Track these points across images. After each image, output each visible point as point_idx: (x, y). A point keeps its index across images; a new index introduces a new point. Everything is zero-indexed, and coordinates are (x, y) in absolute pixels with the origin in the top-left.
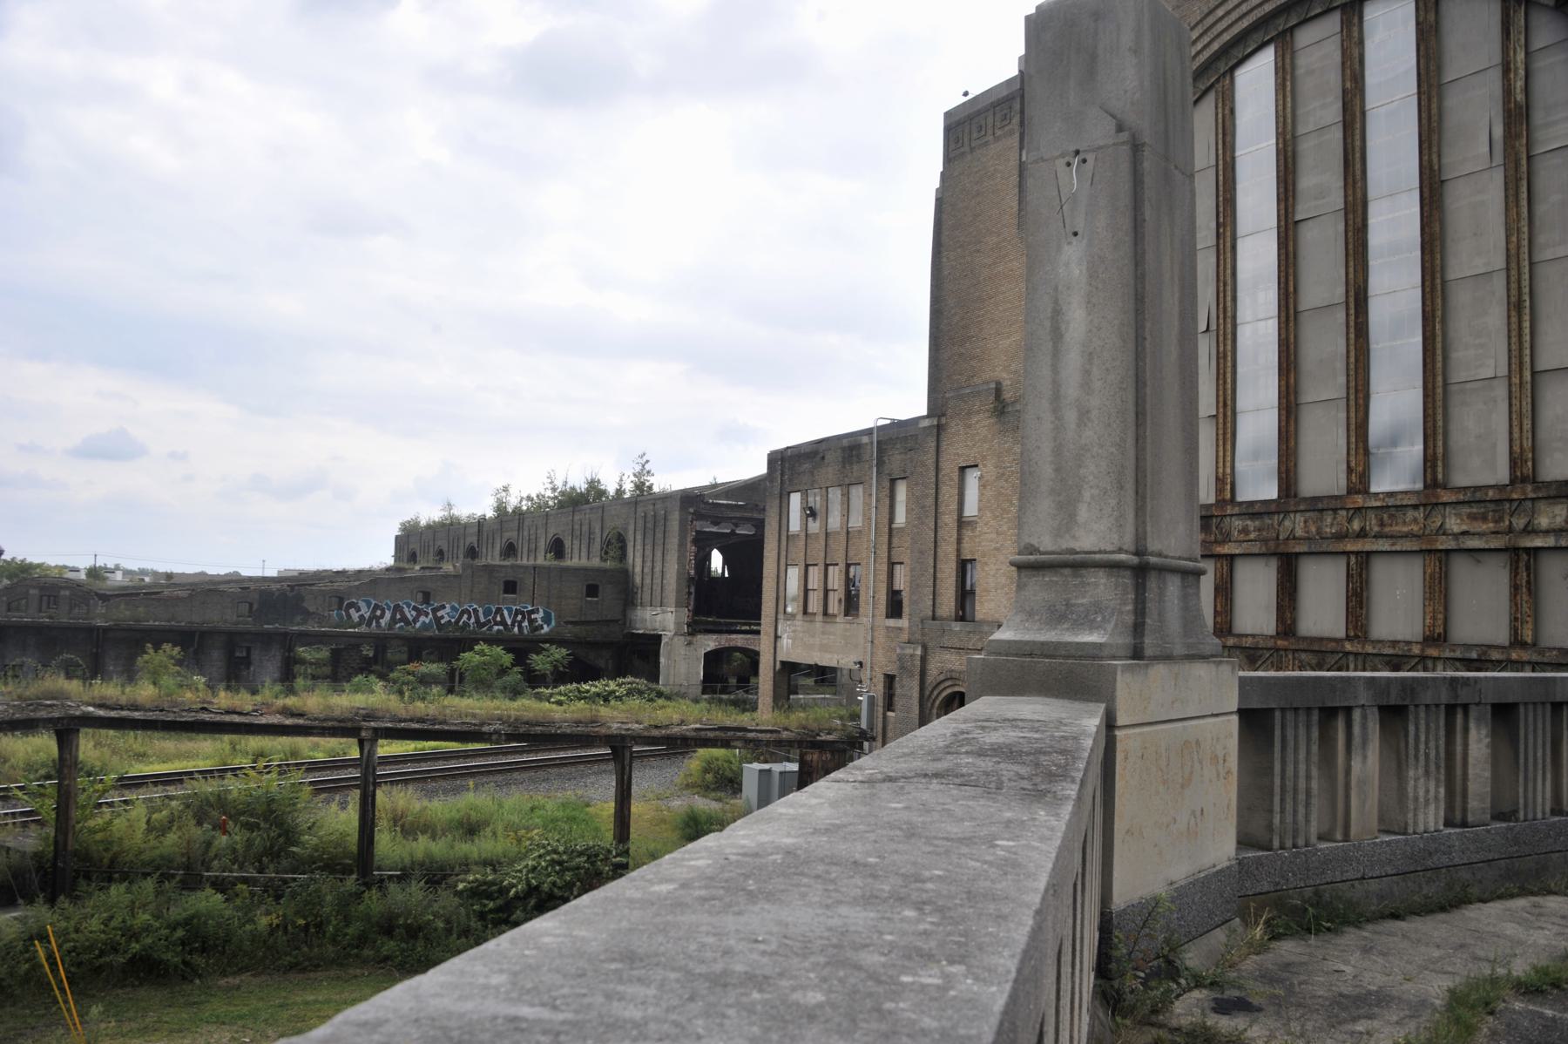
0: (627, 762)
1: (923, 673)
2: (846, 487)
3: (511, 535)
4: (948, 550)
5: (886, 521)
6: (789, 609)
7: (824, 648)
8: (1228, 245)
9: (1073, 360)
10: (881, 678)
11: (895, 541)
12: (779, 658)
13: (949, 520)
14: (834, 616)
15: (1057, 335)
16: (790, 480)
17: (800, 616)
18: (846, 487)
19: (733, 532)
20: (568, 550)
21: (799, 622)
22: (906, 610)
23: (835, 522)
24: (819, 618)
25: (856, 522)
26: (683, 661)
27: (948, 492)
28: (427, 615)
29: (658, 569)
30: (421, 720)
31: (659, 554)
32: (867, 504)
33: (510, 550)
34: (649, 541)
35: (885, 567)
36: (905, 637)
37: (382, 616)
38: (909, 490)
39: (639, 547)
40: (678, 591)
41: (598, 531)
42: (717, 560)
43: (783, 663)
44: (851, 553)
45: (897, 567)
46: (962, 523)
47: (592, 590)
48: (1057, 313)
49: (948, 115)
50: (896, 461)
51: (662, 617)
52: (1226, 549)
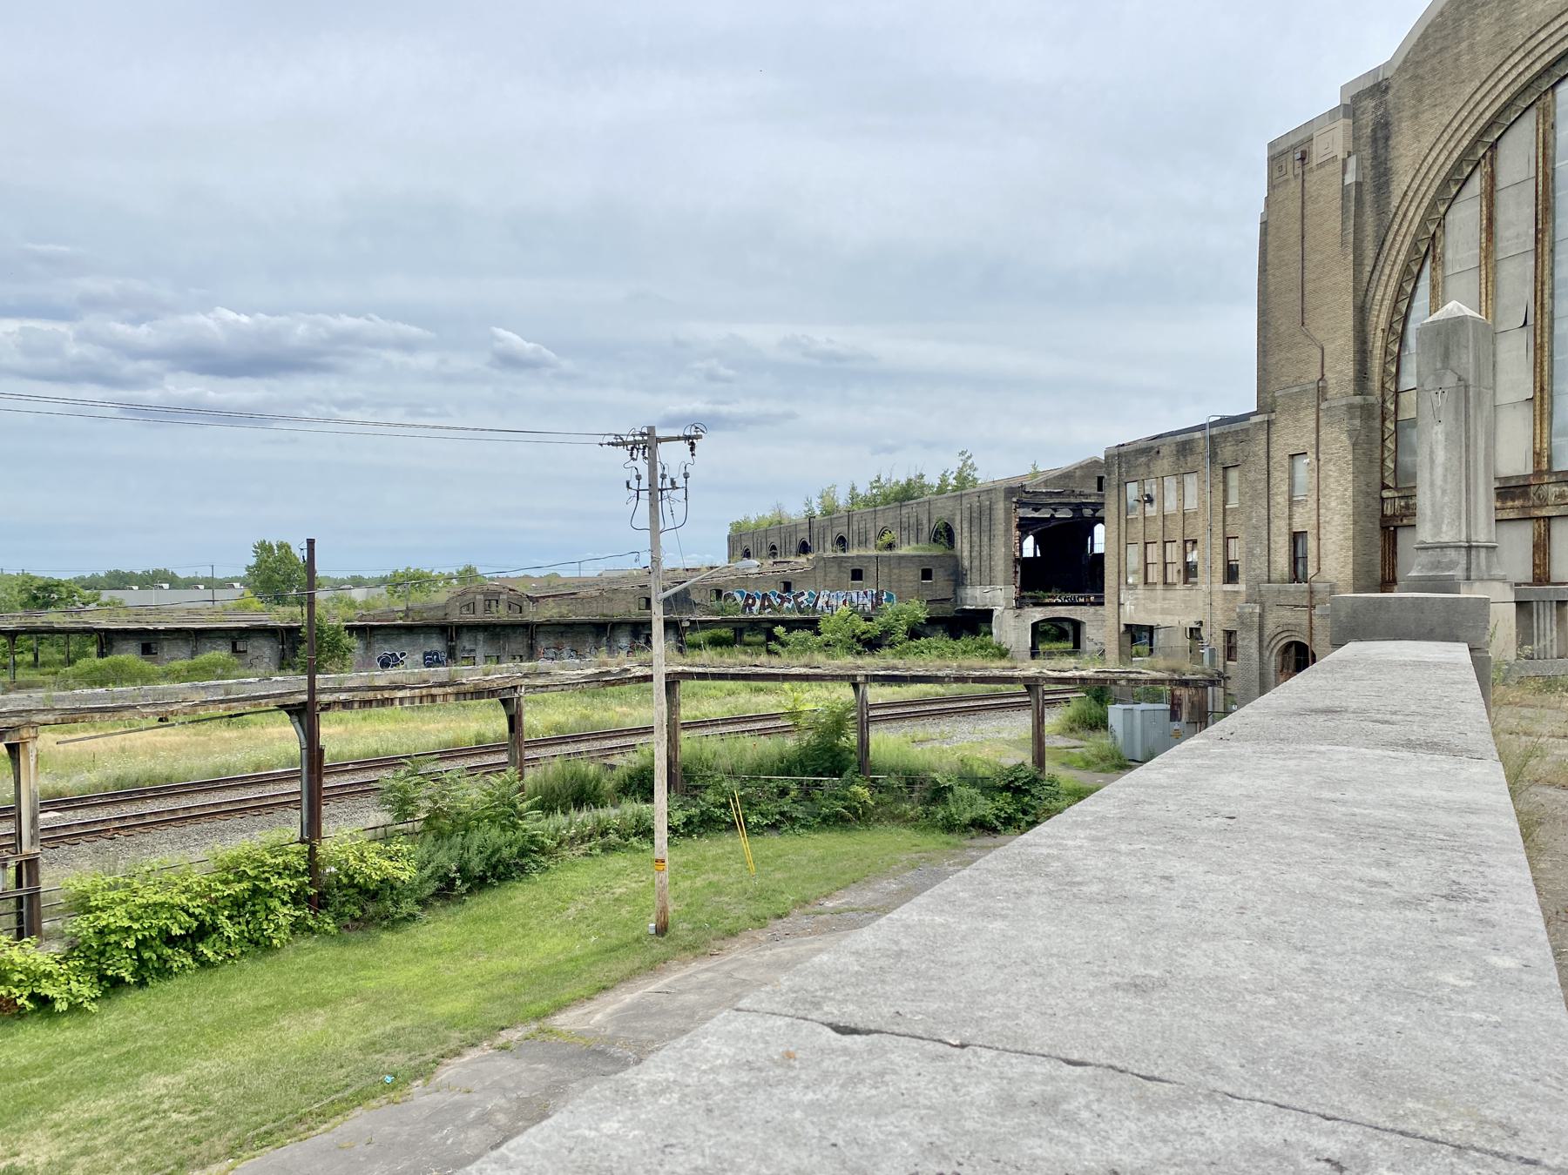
1: (1261, 628)
2: (1180, 475)
6: (1130, 581)
7: (1164, 612)
8: (1547, 249)
11: (1229, 520)
12: (1125, 620)
13: (1281, 500)
17: (1141, 586)
18: (1180, 475)
22: (1242, 576)
23: (1171, 505)
24: (1160, 586)
25: (1191, 503)
27: (1279, 476)
29: (984, 553)
31: (985, 539)
36: (1243, 598)
38: (1242, 476)
39: (966, 534)
40: (1006, 571)
45: (1232, 542)
47: (927, 574)
49: (1271, 145)
50: (1227, 452)
51: (994, 594)
52: (1544, 513)
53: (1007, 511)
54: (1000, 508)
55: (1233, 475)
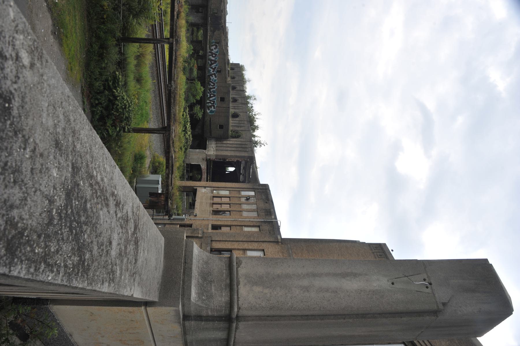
0: (161, 132)
2: (257, 210)
3: (240, 101)
4: (236, 246)
5: (245, 224)
6: (215, 191)
7: (201, 203)
9: (333, 283)
10: (191, 223)
11: (238, 227)
12: (198, 188)
13: (246, 246)
14: (212, 207)
15: (344, 275)
16: (259, 192)
17: (212, 195)
18: (257, 210)
19: (241, 174)
20: (235, 119)
21: (210, 195)
22: (214, 231)
23: (245, 207)
24: (212, 202)
25: (245, 214)
26: (197, 157)
27: (255, 245)
28: (213, 71)
29: (228, 149)
30: (176, 59)
31: (234, 149)
32: (251, 218)
33: (235, 100)
34: (238, 146)
35: (229, 224)
36: (205, 231)
37: (213, 57)
39: (236, 142)
40: (221, 155)
41: (241, 129)
42: (231, 169)
43: (196, 189)
44: (234, 212)
45: (229, 228)
46: (245, 250)
47: (221, 127)
48: (355, 275)
49: (385, 244)
50: (266, 227)
51: (212, 150)
53: (244, 157)
54: (246, 154)
55: (256, 229)
